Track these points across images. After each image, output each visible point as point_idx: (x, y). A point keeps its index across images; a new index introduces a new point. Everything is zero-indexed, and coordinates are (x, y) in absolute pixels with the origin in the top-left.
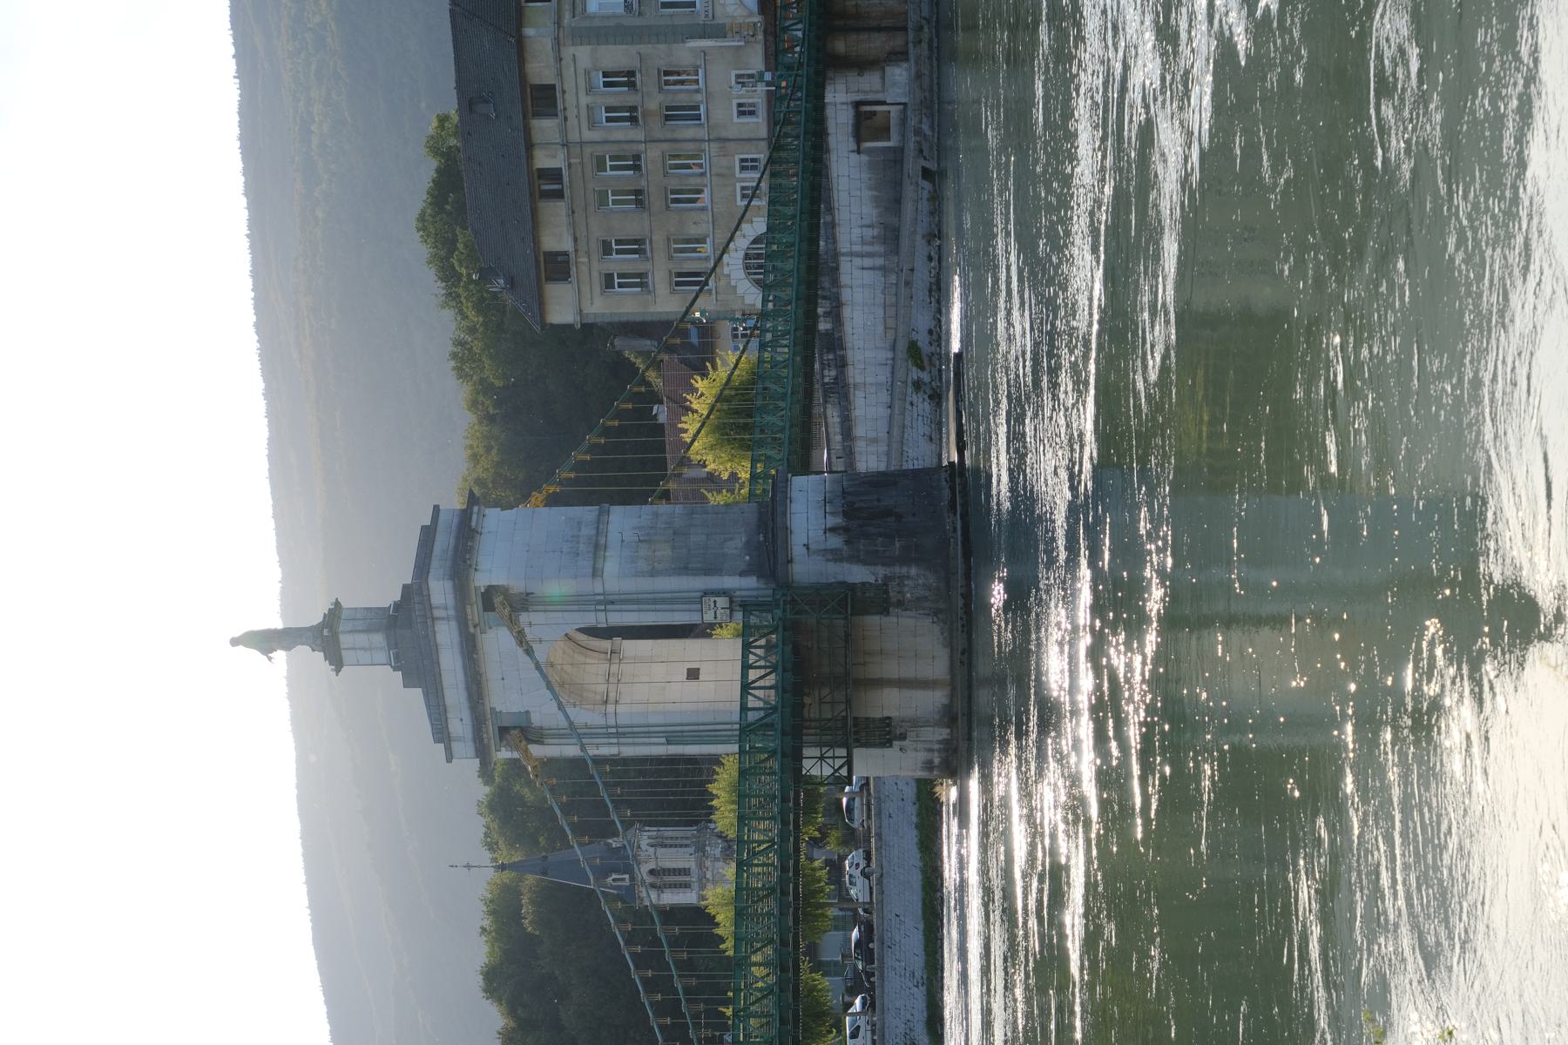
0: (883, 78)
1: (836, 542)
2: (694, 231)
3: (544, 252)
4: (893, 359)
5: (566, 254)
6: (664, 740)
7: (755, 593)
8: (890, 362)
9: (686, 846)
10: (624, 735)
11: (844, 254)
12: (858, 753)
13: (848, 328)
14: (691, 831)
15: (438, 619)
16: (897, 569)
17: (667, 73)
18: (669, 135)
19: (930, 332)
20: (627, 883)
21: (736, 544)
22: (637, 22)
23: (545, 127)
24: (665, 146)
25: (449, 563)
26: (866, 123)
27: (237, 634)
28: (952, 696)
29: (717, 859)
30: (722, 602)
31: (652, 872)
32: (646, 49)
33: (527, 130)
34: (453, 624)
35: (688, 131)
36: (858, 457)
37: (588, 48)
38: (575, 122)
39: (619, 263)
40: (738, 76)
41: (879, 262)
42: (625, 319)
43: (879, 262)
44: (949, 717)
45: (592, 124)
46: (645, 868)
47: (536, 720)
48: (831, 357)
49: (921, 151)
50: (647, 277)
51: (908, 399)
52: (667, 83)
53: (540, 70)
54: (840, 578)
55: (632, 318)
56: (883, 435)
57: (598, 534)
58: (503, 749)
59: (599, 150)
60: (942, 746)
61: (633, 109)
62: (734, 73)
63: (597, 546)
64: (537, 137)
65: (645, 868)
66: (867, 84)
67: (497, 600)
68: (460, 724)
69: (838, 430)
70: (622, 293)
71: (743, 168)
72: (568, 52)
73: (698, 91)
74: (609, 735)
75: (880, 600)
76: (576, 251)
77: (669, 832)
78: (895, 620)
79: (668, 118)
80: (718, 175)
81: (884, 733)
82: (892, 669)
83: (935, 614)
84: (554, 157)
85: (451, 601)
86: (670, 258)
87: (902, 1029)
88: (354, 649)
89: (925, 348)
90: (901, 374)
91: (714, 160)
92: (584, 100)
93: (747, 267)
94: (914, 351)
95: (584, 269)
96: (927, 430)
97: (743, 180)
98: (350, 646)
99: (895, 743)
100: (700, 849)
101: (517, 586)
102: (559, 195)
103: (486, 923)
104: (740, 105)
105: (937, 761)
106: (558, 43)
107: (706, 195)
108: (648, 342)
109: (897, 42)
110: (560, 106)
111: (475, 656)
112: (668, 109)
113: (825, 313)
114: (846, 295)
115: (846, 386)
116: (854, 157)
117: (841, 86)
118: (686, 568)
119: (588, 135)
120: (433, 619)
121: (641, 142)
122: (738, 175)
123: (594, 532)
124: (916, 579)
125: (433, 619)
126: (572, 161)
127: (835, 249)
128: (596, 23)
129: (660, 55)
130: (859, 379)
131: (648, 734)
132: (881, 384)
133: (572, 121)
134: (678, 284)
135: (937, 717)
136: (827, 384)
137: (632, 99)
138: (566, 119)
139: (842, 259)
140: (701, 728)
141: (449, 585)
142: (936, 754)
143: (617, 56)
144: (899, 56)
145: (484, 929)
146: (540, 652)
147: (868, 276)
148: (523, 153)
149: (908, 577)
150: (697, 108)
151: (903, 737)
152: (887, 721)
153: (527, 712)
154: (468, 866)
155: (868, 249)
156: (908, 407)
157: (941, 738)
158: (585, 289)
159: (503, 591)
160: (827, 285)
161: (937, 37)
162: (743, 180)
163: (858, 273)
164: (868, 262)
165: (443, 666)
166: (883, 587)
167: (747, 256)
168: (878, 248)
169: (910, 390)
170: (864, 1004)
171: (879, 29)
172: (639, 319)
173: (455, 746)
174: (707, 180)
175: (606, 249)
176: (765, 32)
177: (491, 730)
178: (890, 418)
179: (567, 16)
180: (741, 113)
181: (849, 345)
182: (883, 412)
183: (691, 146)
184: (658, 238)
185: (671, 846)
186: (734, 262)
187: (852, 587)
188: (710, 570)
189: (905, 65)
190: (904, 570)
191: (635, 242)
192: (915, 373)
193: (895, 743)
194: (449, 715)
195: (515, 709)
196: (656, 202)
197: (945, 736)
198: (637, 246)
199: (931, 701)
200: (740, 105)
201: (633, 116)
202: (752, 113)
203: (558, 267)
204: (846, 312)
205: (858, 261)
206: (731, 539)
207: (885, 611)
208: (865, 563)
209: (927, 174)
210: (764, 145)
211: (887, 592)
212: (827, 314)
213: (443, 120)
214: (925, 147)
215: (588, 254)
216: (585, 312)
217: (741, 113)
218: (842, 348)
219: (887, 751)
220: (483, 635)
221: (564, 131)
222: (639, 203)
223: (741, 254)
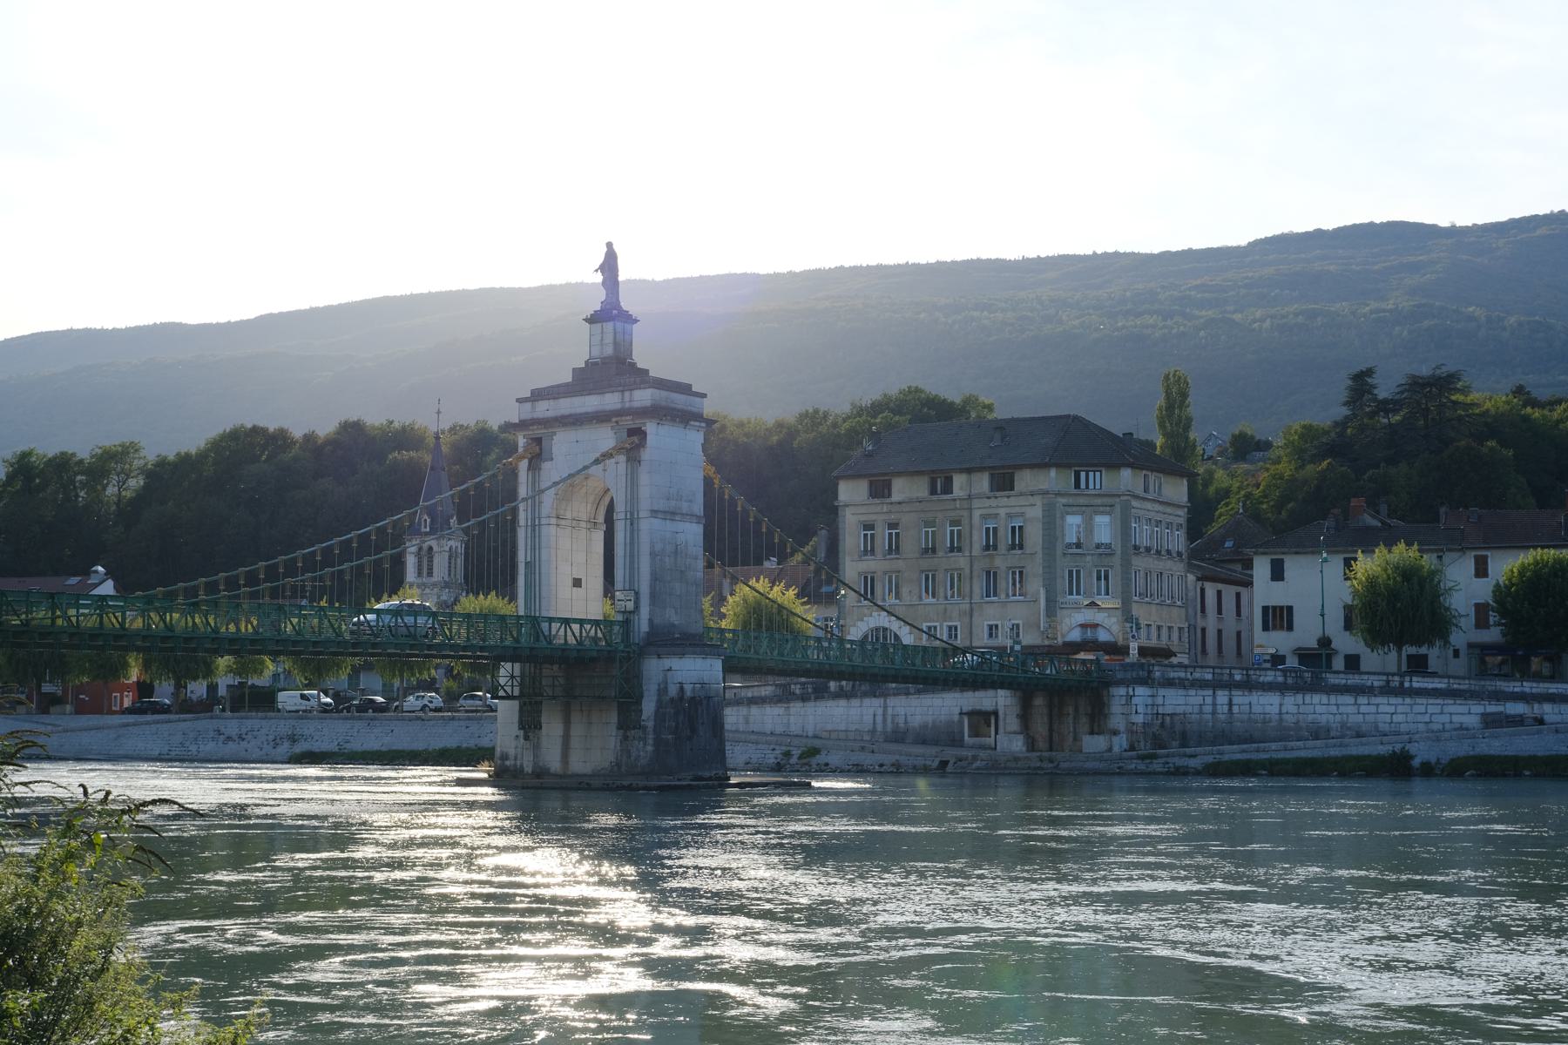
0: (1015, 733)
1: (673, 691)
2: (904, 590)
3: (890, 481)
4: (807, 737)
5: (890, 495)
6: (529, 559)
7: (636, 629)
9: (450, 575)
10: (534, 530)
11: (885, 701)
12: (516, 703)
13: (831, 703)
14: (460, 578)
15: (623, 395)
16: (651, 736)
17: (1021, 573)
18: (975, 574)
19: (827, 764)
20: (423, 530)
21: (672, 617)
22: (1059, 552)
23: (983, 482)
24: (967, 571)
25: (664, 403)
26: (982, 720)
27: (615, 247)
28: (556, 775)
29: (439, 597)
30: (630, 606)
31: (431, 548)
32: (1039, 557)
33: (981, 469)
34: (619, 406)
35: (978, 587)
36: (735, 708)
38: (987, 505)
39: (882, 535)
40: (1018, 625)
41: (879, 728)
42: (841, 537)
43: (879, 728)
44: (540, 773)
45: (984, 517)
46: (433, 543)
47: (546, 466)
48: (810, 690)
51: (777, 747)
52: (1014, 573)
53: (1025, 480)
54: (646, 694)
55: (841, 543)
57: (683, 514)
59: (965, 522)
61: (995, 547)
62: (1020, 622)
63: (673, 513)
64: (975, 477)
65: (433, 543)
66: (1011, 722)
67: (636, 439)
68: (544, 409)
69: (756, 694)
70: (860, 537)
71: (950, 628)
72: (1038, 500)
73: (1007, 595)
74: (533, 520)
75: (628, 721)
76: (892, 503)
77: (460, 561)
78: (614, 734)
79: (988, 573)
80: (946, 610)
81: (529, 724)
82: (577, 730)
83: (617, 764)
84: (961, 489)
85: (636, 404)
86: (885, 573)
87: (306, 732)
88: (602, 333)
89: (814, 761)
90: (796, 741)
92: (1002, 512)
93: (877, 629)
94: (814, 752)
95: (878, 509)
96: (754, 760)
97: (941, 628)
100: (447, 585)
101: (646, 455)
102: (933, 492)
103: (396, 424)
104: (997, 626)
105: (508, 763)
106: (1045, 493)
107: (931, 600)
109: (1042, 744)
110: (998, 494)
112: (995, 573)
113: (843, 686)
114: (855, 702)
115: (788, 701)
116: (957, 710)
117: (1009, 701)
118: (656, 580)
119: (977, 514)
122: (945, 624)
123: (684, 512)
124: (644, 750)
125: (623, 391)
126: (958, 502)
127: (889, 695)
128: (1058, 522)
129: (1035, 568)
130: (793, 710)
133: (988, 503)
134: (866, 578)
135: (541, 764)
137: (1002, 547)
138: (989, 498)
139: (882, 700)
140: (537, 588)
141: (648, 403)
142: (513, 762)
143: (1034, 537)
144: (1031, 745)
145: (392, 422)
146: (596, 470)
147: (868, 719)
148: (964, 466)
149: (645, 744)
150: (1078, 593)
151: (526, 738)
152: (538, 726)
153: (552, 459)
154: (439, 412)
156: (772, 747)
158: (863, 510)
159: (642, 444)
160: (863, 688)
161: (1045, 774)
163: (871, 711)
164: (879, 719)
165: (587, 398)
166: (638, 726)
167: (885, 629)
169: (784, 748)
170: (326, 704)
171: (1051, 730)
172: (840, 549)
173: (528, 405)
174: (942, 600)
175: (892, 526)
176: (1049, 646)
177: (538, 431)
179: (1064, 500)
180: (991, 627)
181: (818, 704)
182: (768, 728)
183: (967, 589)
184: (900, 564)
185: (450, 563)
186: (881, 620)
187: (639, 702)
188: (653, 596)
189: (1024, 749)
190: (651, 742)
191: (897, 547)
192: (796, 752)
193: (521, 733)
195: (554, 450)
196: (926, 563)
198: (894, 549)
199: (552, 759)
200: (997, 626)
202: (991, 635)
203: (880, 490)
204: (843, 702)
205: (880, 711)
206: (676, 613)
207: (620, 727)
208: (657, 712)
209: (944, 764)
211: (634, 728)
212: (841, 688)
213: (990, 408)
214: (964, 763)
215: (890, 512)
217: (991, 627)
218: (816, 699)
219: (516, 726)
221: (980, 496)
222: (926, 550)
223: (887, 625)
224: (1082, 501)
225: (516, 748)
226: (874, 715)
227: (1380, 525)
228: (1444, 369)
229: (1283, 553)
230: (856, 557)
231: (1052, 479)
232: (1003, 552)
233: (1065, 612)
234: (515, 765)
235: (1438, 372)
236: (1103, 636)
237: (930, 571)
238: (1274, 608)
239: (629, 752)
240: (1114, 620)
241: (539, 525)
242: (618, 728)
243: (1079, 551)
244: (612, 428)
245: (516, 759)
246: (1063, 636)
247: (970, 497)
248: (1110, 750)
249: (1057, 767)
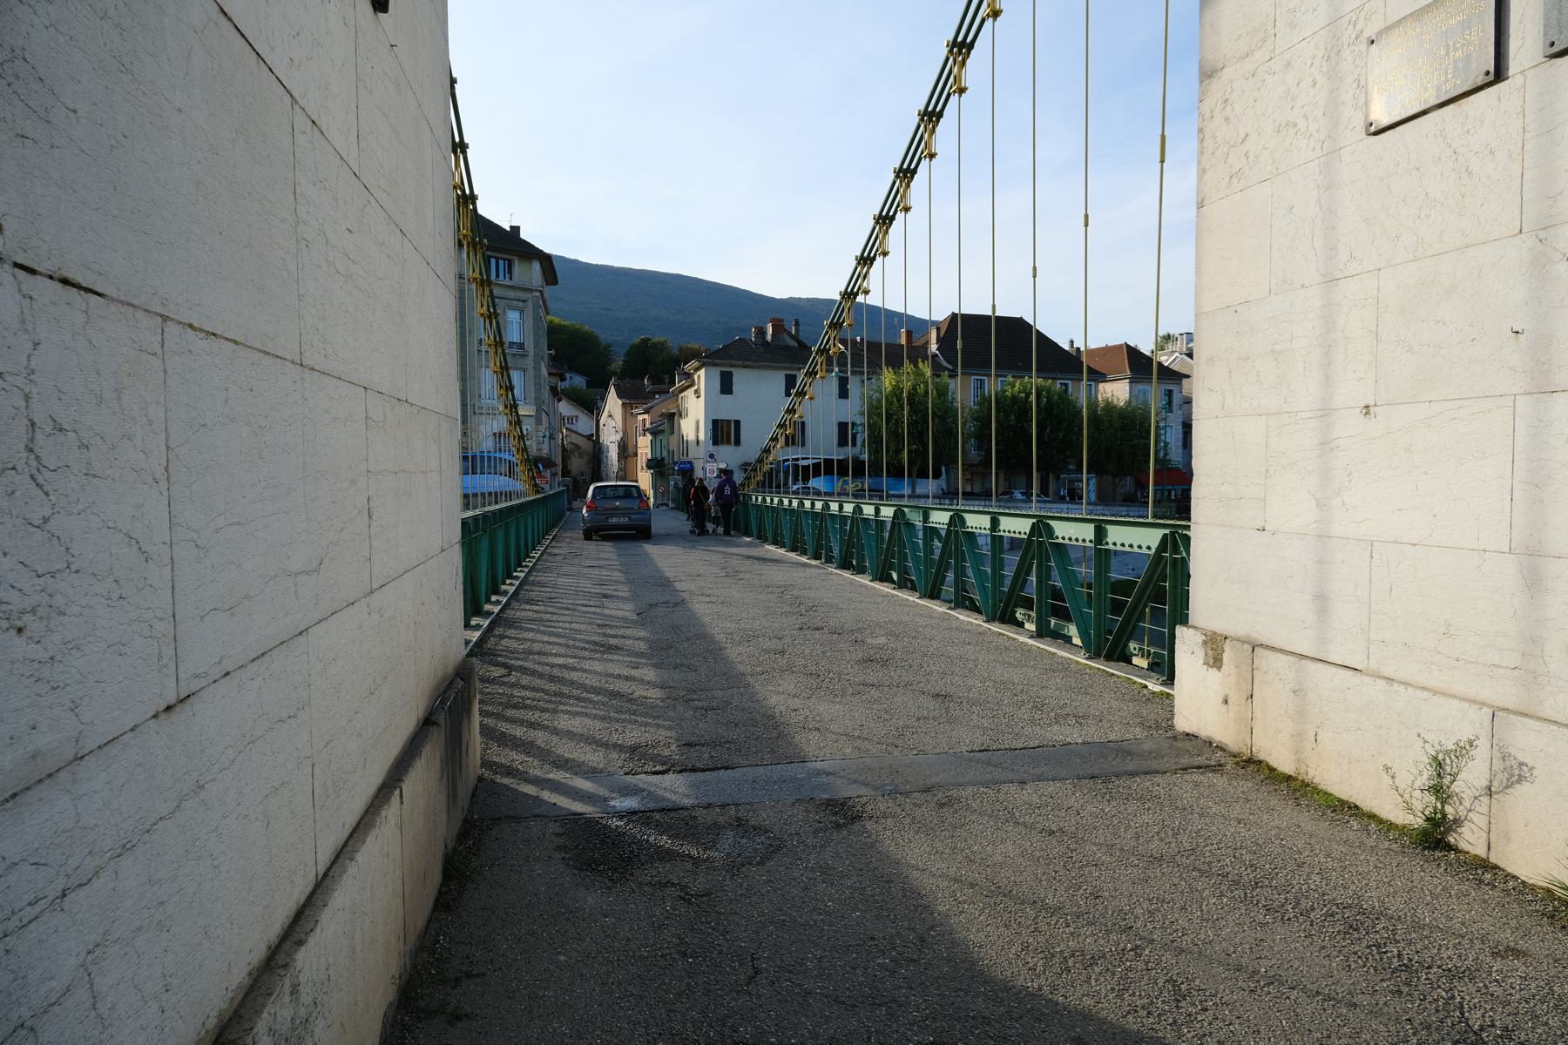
227: (796, 345)
229: (732, 366)
238: (722, 421)
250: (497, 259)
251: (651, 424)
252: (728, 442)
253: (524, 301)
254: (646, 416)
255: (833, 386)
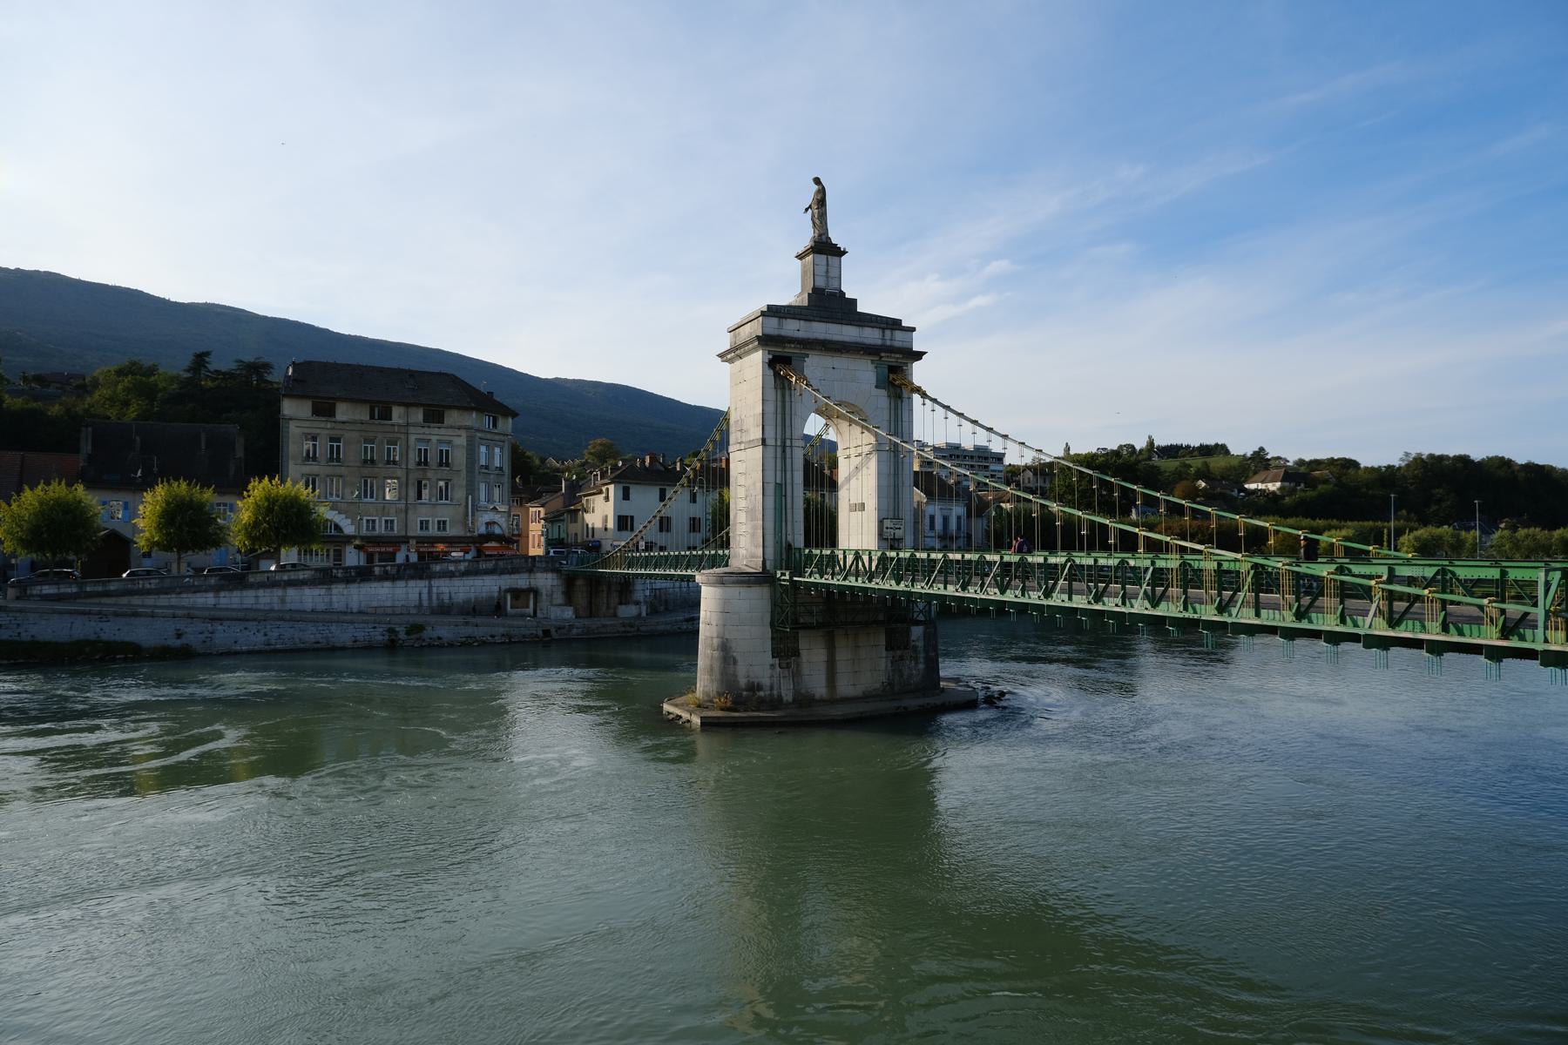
0: (560, 605)
3: (334, 404)
8: (349, 610)
10: (784, 451)
11: (430, 583)
13: (375, 585)
15: (884, 332)
16: (922, 655)
18: (410, 482)
22: (477, 472)
23: (418, 415)
30: (899, 533)
32: (464, 472)
33: (417, 405)
34: (879, 342)
36: (269, 590)
37: (465, 444)
40: (444, 522)
41: (425, 603)
43: (425, 603)
44: (804, 700)
49: (559, 628)
50: (313, 461)
56: (288, 607)
58: (771, 357)
60: (776, 697)
61: (426, 463)
64: (412, 410)
68: (792, 328)
69: (292, 577)
71: (386, 521)
72: (463, 433)
74: (784, 442)
76: (334, 422)
78: (884, 655)
82: (843, 655)
83: (889, 684)
85: (897, 344)
88: (828, 265)
91: (394, 506)
92: (434, 438)
95: (322, 425)
97: (380, 521)
98: (830, 263)
99: (777, 661)
102: (372, 417)
104: (427, 522)
108: (90, 448)
110: (432, 425)
111: (862, 352)
113: (387, 571)
114: (401, 584)
116: (496, 589)
117: (555, 583)
119: (412, 438)
120: (883, 329)
121: (407, 465)
126: (396, 428)
127: (435, 578)
128: (477, 449)
130: (334, 591)
131: (784, 470)
132: (331, 605)
133: (422, 430)
135: (803, 691)
136: (332, 572)
140: (789, 511)
142: (768, 693)
143: (459, 458)
147: (414, 597)
149: (917, 663)
152: (796, 653)
155: (434, 597)
157: (783, 695)
158: (307, 424)
160: (408, 572)
162: (380, 521)
163: (417, 590)
164: (425, 596)
168: (435, 602)
171: (590, 603)
173: (774, 321)
174: (380, 500)
177: (789, 350)
178: (304, 612)
179: (479, 435)
181: (362, 585)
182: (308, 606)
184: (343, 470)
189: (574, 617)
190: (922, 660)
193: (777, 661)
194: (802, 322)
196: (366, 471)
197: (785, 699)
199: (816, 683)
200: (427, 522)
201: (423, 463)
203: (324, 409)
204: (387, 584)
205: (425, 591)
207: (889, 647)
210: (403, 533)
212: (386, 572)
215: (333, 429)
216: (291, 422)
217: (422, 522)
218: (362, 581)
220: (869, 362)
221: (416, 425)
222: (365, 461)
224: (489, 436)
225: (772, 676)
226: (420, 594)
228: (262, 360)
229: (630, 483)
230: (300, 462)
231: (472, 419)
232: (435, 468)
233: (479, 513)
234: (771, 695)
235: (257, 361)
236: (497, 531)
237: (310, 475)
239: (900, 671)
240: (504, 519)
241: (791, 446)
242: (886, 649)
243: (486, 471)
244: (873, 362)
245: (772, 688)
246: (478, 530)
247: (408, 425)
248: (640, 614)
249: (638, 630)
250: (489, 416)
251: (546, 514)
252: (626, 529)
253: (503, 442)
254: (541, 509)
255: (687, 496)
